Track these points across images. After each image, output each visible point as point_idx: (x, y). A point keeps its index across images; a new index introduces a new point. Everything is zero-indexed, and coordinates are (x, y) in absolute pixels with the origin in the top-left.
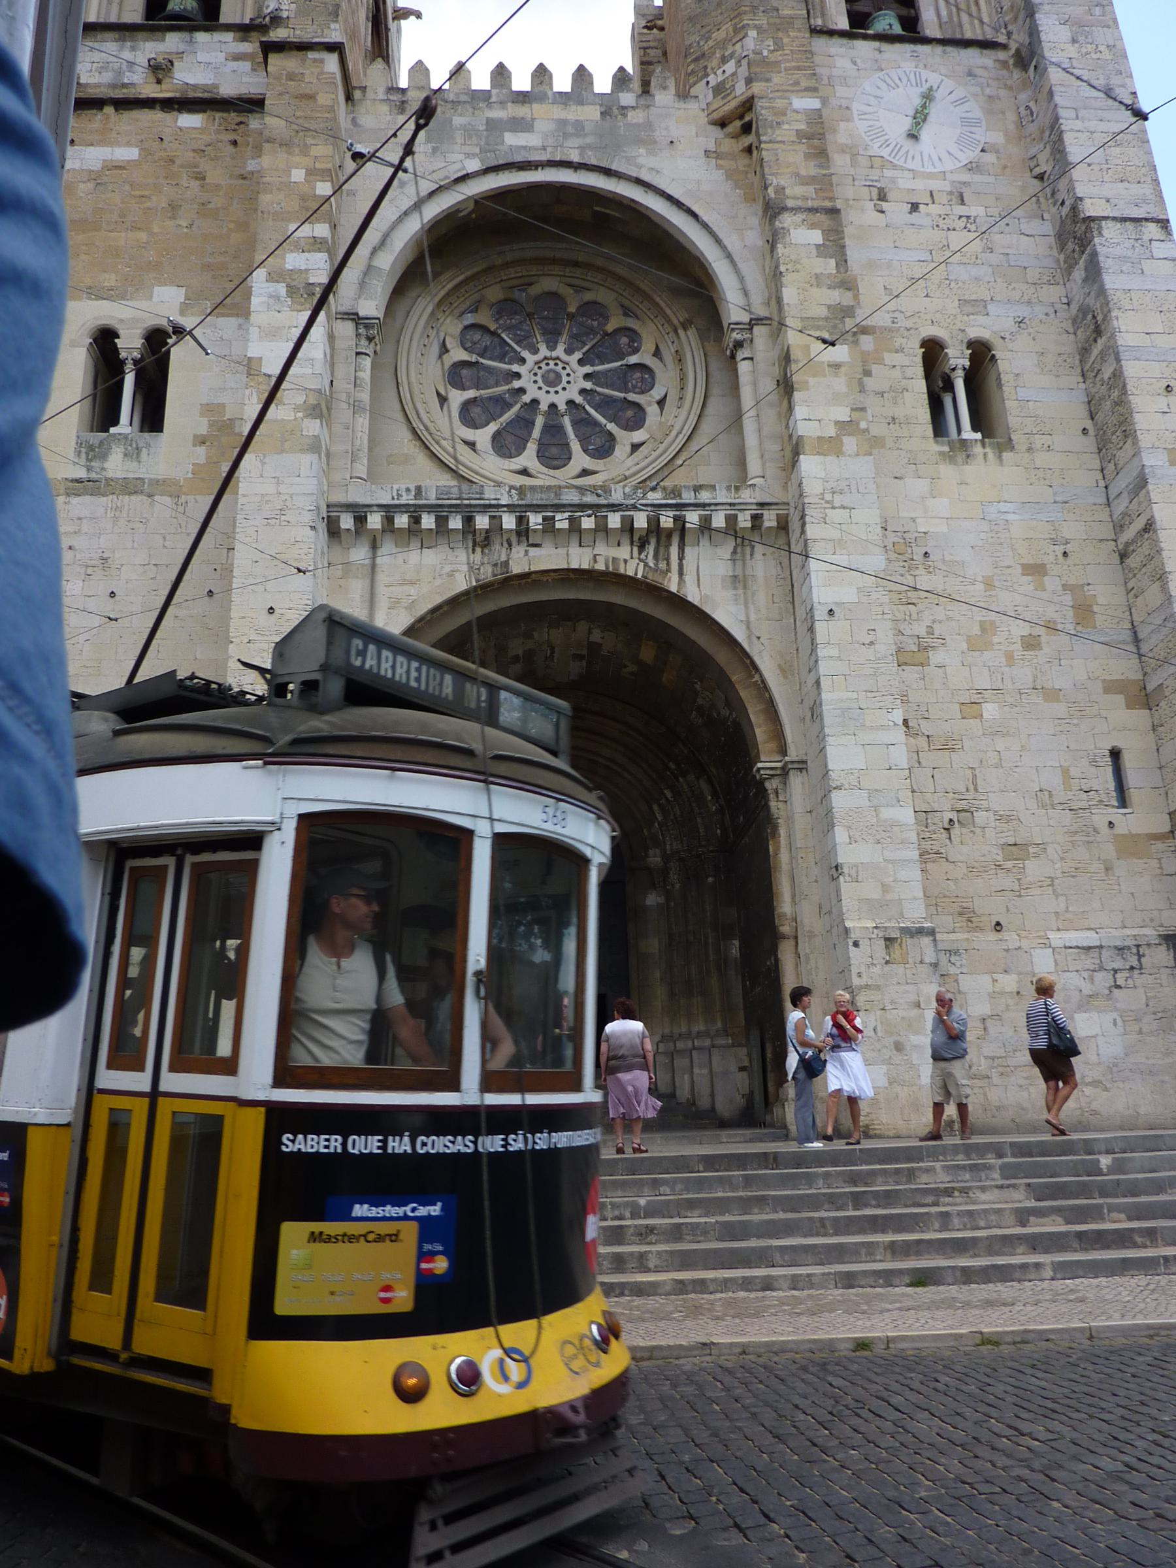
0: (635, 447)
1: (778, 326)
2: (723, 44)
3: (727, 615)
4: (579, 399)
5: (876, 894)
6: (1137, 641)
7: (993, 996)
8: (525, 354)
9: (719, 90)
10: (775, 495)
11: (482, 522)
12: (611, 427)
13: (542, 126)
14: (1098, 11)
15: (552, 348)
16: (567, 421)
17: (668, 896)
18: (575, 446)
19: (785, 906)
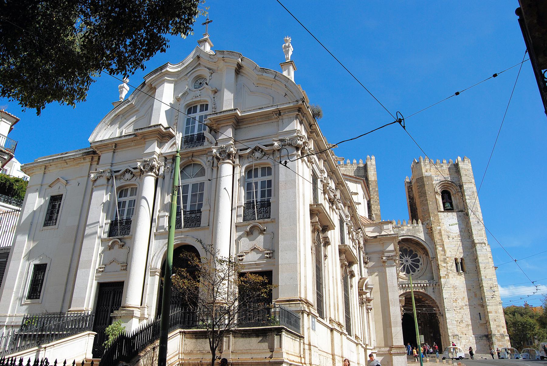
0: (418, 271)
1: (437, 260)
2: (427, 217)
3: (433, 296)
4: (411, 264)
5: (452, 331)
6: (482, 299)
7: (465, 342)
8: (403, 258)
9: (427, 224)
10: (438, 281)
11: (404, 286)
12: (415, 268)
13: (405, 230)
14: (477, 209)
15: (406, 257)
16: (409, 267)
17: (422, 327)
18: (411, 271)
19: (441, 332)
